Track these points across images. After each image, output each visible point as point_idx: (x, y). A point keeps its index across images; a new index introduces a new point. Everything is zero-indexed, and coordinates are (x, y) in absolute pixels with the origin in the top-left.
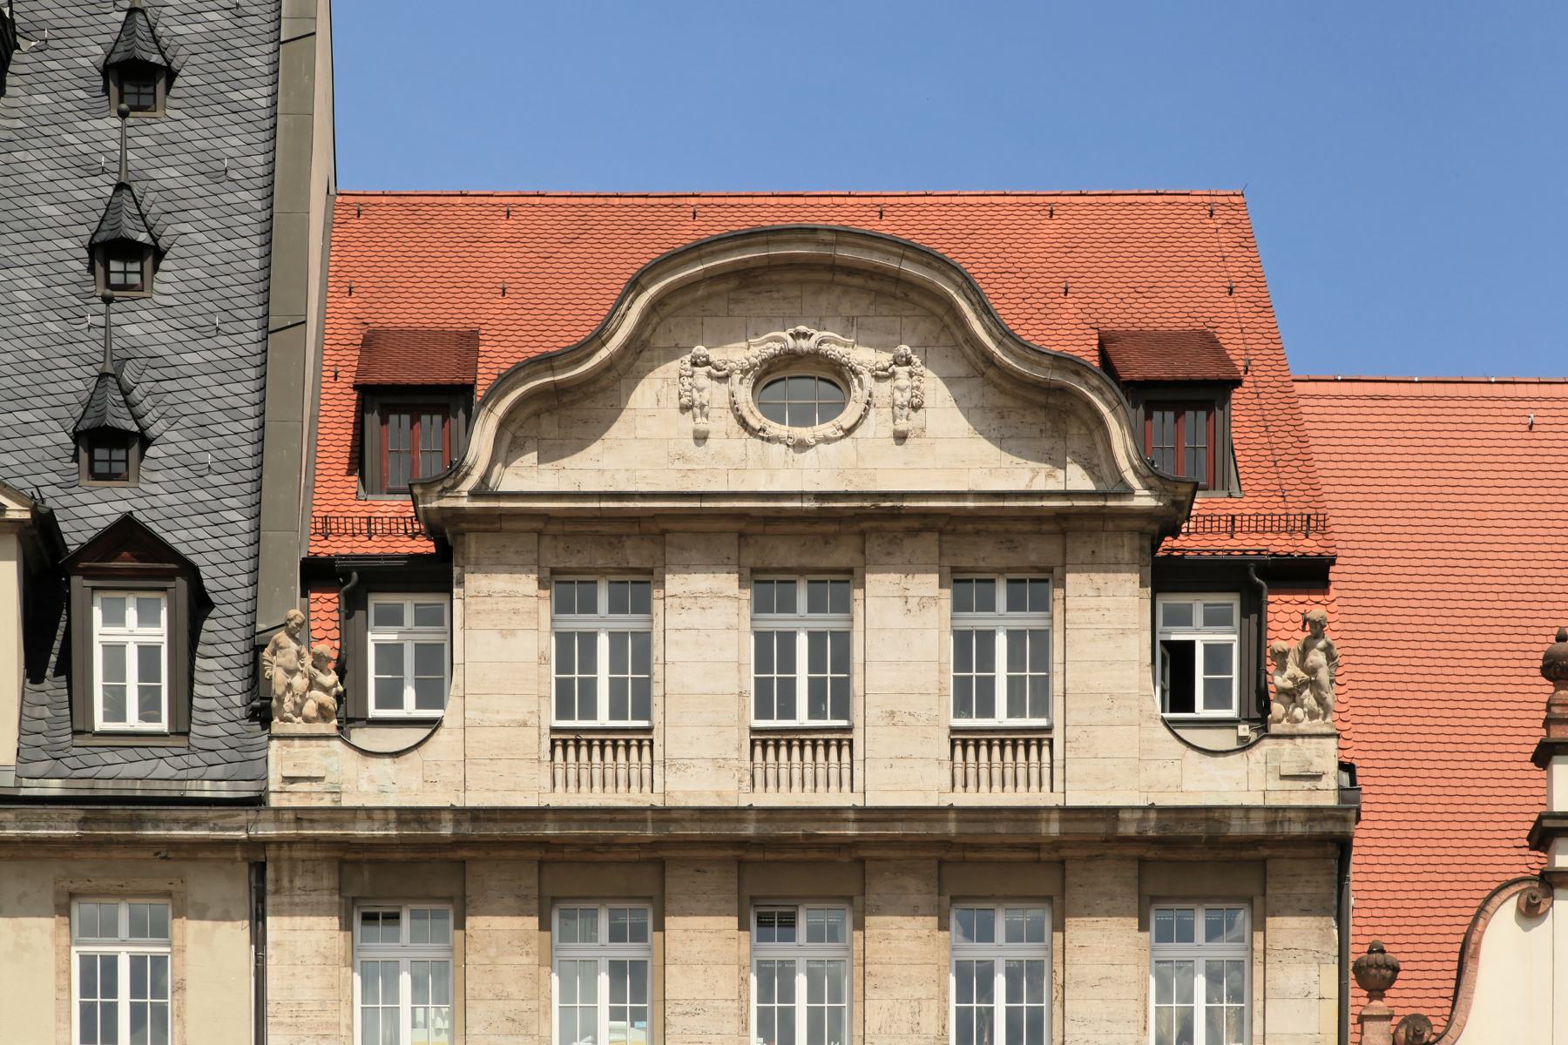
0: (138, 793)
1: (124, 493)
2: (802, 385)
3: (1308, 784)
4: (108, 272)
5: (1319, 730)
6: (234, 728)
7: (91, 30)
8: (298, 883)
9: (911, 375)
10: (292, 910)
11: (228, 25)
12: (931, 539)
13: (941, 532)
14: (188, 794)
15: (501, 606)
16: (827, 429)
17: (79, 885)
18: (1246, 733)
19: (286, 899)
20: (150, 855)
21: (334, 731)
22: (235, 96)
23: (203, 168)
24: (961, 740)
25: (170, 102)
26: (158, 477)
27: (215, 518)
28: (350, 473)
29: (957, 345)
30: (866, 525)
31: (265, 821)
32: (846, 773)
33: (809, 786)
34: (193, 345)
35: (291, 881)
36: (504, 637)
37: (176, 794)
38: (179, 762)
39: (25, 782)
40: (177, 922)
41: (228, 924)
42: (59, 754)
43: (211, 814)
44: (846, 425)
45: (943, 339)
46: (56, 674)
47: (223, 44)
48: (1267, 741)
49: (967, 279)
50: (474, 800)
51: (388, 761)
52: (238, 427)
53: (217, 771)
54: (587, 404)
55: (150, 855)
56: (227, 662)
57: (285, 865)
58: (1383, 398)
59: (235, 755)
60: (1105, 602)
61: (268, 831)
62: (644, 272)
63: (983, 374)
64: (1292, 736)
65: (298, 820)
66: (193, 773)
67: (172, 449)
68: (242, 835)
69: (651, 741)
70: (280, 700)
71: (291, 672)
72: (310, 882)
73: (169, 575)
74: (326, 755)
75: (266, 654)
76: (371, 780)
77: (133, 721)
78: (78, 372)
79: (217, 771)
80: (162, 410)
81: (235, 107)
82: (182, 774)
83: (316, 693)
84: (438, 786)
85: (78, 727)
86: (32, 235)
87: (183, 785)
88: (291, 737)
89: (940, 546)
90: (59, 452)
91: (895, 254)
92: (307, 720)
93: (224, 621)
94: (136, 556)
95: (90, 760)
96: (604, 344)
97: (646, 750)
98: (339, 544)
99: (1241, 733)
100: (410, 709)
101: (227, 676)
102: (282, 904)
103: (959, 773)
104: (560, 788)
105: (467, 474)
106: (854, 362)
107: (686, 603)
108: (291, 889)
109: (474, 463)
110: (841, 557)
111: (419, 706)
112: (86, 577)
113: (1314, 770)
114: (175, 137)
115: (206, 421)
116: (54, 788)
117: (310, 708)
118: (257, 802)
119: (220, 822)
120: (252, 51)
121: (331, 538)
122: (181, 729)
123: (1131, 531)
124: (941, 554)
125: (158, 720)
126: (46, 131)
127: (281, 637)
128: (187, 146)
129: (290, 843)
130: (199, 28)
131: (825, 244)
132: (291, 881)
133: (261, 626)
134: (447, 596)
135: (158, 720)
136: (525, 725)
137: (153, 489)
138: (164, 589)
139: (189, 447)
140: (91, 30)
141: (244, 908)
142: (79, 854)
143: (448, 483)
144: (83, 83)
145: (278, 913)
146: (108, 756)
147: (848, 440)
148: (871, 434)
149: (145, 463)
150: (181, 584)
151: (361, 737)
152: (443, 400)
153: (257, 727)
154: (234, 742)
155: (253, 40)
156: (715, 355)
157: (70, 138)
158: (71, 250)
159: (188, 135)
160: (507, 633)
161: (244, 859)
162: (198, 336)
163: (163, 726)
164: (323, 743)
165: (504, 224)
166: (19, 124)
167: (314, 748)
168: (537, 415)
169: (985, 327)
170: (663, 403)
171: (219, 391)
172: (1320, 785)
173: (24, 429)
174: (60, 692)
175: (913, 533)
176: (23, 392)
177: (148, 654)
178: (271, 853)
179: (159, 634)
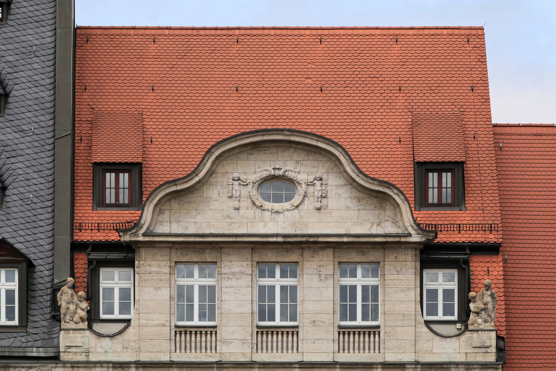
0: (7, 354)
2: (278, 185)
3: (484, 350)
5: (488, 328)
6: (45, 323)
9: (322, 184)
12: (330, 252)
13: (334, 248)
15: (155, 277)
16: (287, 205)
18: (460, 327)
21: (86, 327)
24: (343, 331)
29: (340, 172)
30: (303, 246)
31: (59, 367)
32: (295, 345)
33: (280, 351)
36: (156, 290)
37: (22, 355)
38: (24, 339)
43: (37, 365)
44: (296, 205)
45: (335, 170)
48: (467, 332)
49: (344, 149)
50: (144, 357)
51: (108, 339)
53: (39, 343)
54: (190, 195)
58: (540, 135)
60: (401, 277)
62: (213, 147)
63: (351, 184)
64: (477, 331)
66: (29, 344)
69: (216, 332)
73: (20, 262)
74: (83, 337)
75: (59, 293)
76: (102, 347)
79: (39, 343)
80: (10, 172)
82: (24, 345)
84: (129, 350)
87: (25, 350)
88: (69, 330)
89: (334, 254)
91: (315, 140)
92: (76, 323)
96: (197, 175)
97: (214, 335)
99: (458, 327)
100: (116, 315)
103: (341, 345)
104: (178, 351)
105: (141, 227)
106: (298, 180)
107: (230, 277)
109: (145, 223)
110: (293, 257)
111: (120, 314)
113: (486, 345)
117: (76, 318)
121: (83, 231)
123: (412, 248)
124: (334, 257)
131: (287, 135)
133: (56, 281)
134: (131, 270)
136: (164, 326)
143: (134, 231)
147: (296, 211)
148: (306, 208)
150: (24, 265)
151: (97, 327)
152: (129, 167)
156: (243, 177)
160: (157, 289)
162: (24, 135)
163: (16, 322)
164: (82, 332)
165: (153, 47)
167: (78, 335)
168: (170, 200)
169: (352, 169)
170: (221, 195)
172: (489, 350)
175: (323, 249)
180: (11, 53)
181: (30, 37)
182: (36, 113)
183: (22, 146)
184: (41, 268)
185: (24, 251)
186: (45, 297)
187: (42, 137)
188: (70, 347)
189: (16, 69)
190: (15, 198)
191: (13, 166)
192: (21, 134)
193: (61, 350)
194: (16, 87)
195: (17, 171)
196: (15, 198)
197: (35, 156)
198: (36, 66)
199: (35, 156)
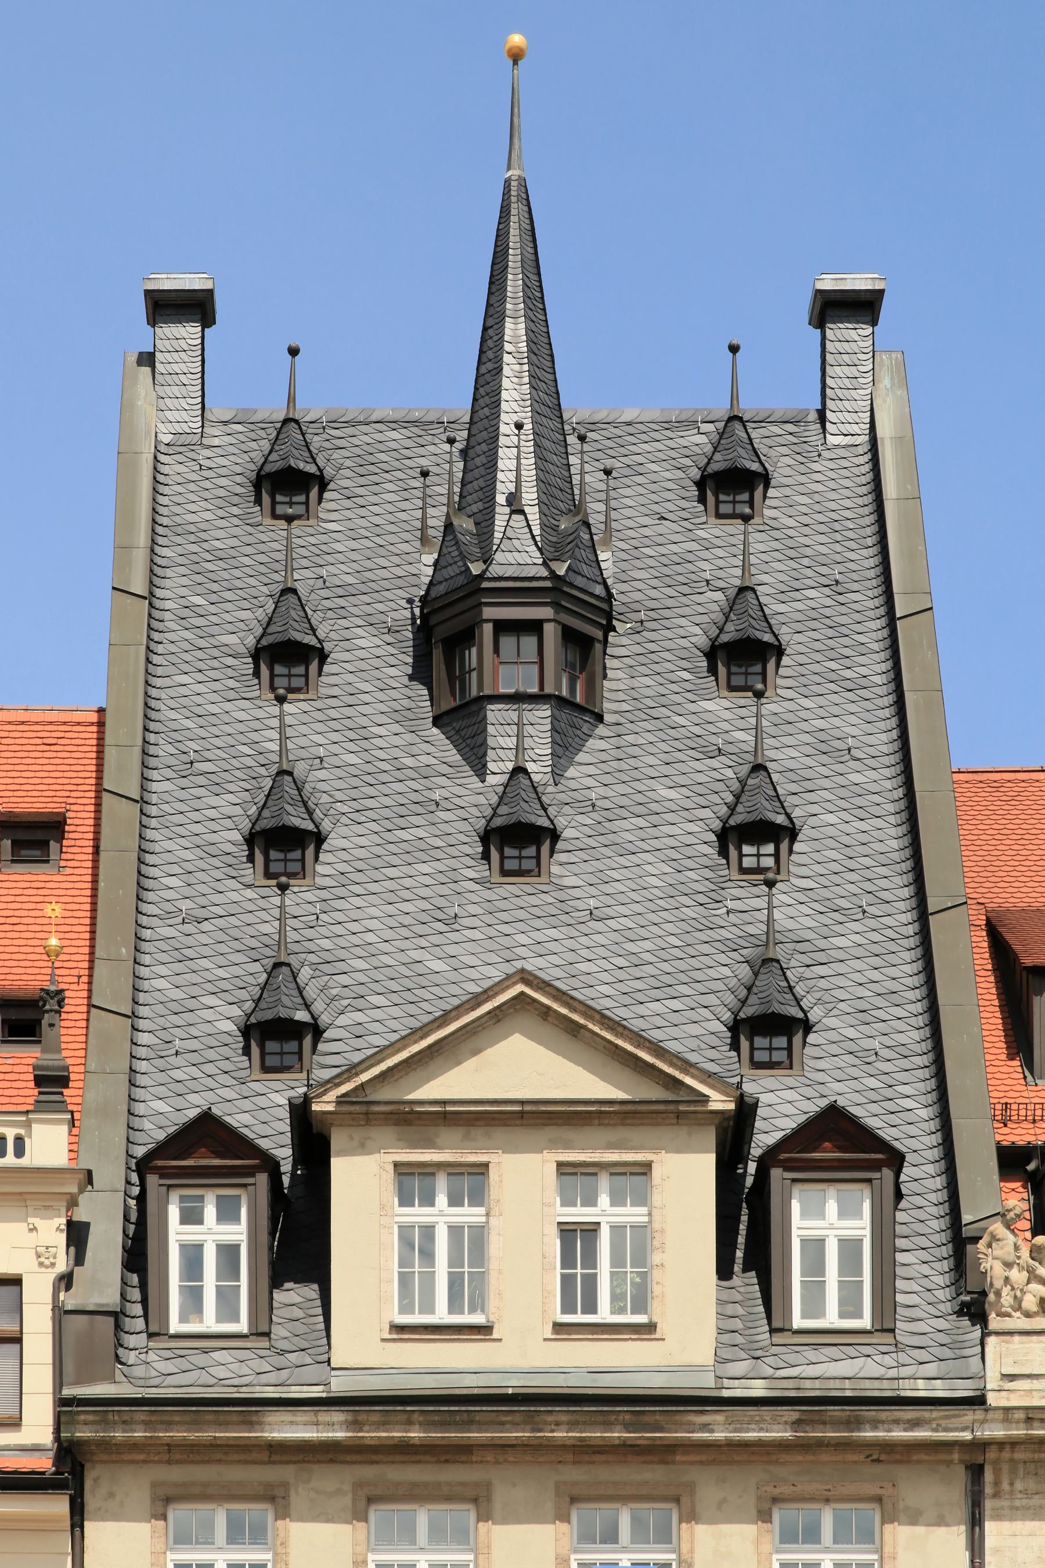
0: (848, 1393)
1: (790, 1081)
4: (741, 856)
6: (941, 1324)
7: (687, 611)
8: (1019, 1486)
10: (1015, 1513)
11: (829, 602)
14: (903, 1394)
17: (785, 1490)
19: (1006, 1503)
20: (862, 1457)
22: (848, 674)
23: (824, 747)
25: (780, 681)
26: (821, 1064)
27: (890, 1106)
28: (1011, 1057)
34: (838, 928)
35: (1012, 1484)
38: (888, 1360)
39: (726, 1383)
40: (888, 1528)
41: (942, 1530)
42: (759, 1353)
43: (935, 1414)
46: (745, 1270)
47: (827, 622)
52: (899, 1012)
55: (862, 1457)
56: (924, 1255)
57: (1005, 1468)
59: (947, 1353)
61: (996, 1431)
65: (1029, 1420)
66: (905, 1372)
67: (833, 1036)
68: (967, 1436)
70: (998, 1294)
71: (1008, 1265)
72: (1032, 1484)
77: (832, 1319)
78: (723, 958)
79: (931, 1369)
80: (818, 995)
81: (849, 685)
83: (1034, 1286)
85: (776, 1324)
86: (655, 819)
87: (895, 1384)
88: (1011, 1333)
90: (714, 1041)
92: (1028, 1315)
93: (915, 1213)
94: (840, 1144)
95: (791, 1358)
98: (1019, 1131)
101: (926, 1270)
102: (1002, 1508)
108: (1012, 1492)
112: (787, 1169)
114: (790, 717)
115: (865, 1006)
116: (758, 1389)
117: (1030, 1303)
118: (978, 1401)
119: (943, 1423)
120: (858, 628)
121: (1010, 1125)
122: (885, 1324)
125: (859, 1315)
126: (654, 713)
127: (997, 1227)
128: (804, 726)
129: (1013, 1444)
130: (799, 606)
132: (1012, 1484)
133: (966, 1218)
135: (861, 1317)
137: (820, 1077)
138: (869, 1181)
139: (851, 1033)
140: (687, 611)
141: (962, 1510)
142: (785, 1457)
144: (685, 664)
145: (998, 1517)
146: (811, 1354)
149: (808, 1050)
153: (966, 1322)
154: (943, 1338)
155: (858, 617)
157: (681, 720)
158: (698, 834)
159: (804, 714)
161: (961, 1461)
163: (865, 1322)
166: (625, 707)
171: (875, 975)
173: (675, 1018)
174: (750, 1289)
176: (668, 980)
177: (849, 1248)
178: (992, 1454)
179: (861, 1227)
181: (836, 721)
183: (838, 941)
185: (887, 1134)
186: (937, 1265)
187: (887, 921)
188: (1012, 1377)
189: (809, 785)
191: (823, 984)
192: (836, 916)
193: (988, 1387)
194: (812, 821)
195: (832, 992)
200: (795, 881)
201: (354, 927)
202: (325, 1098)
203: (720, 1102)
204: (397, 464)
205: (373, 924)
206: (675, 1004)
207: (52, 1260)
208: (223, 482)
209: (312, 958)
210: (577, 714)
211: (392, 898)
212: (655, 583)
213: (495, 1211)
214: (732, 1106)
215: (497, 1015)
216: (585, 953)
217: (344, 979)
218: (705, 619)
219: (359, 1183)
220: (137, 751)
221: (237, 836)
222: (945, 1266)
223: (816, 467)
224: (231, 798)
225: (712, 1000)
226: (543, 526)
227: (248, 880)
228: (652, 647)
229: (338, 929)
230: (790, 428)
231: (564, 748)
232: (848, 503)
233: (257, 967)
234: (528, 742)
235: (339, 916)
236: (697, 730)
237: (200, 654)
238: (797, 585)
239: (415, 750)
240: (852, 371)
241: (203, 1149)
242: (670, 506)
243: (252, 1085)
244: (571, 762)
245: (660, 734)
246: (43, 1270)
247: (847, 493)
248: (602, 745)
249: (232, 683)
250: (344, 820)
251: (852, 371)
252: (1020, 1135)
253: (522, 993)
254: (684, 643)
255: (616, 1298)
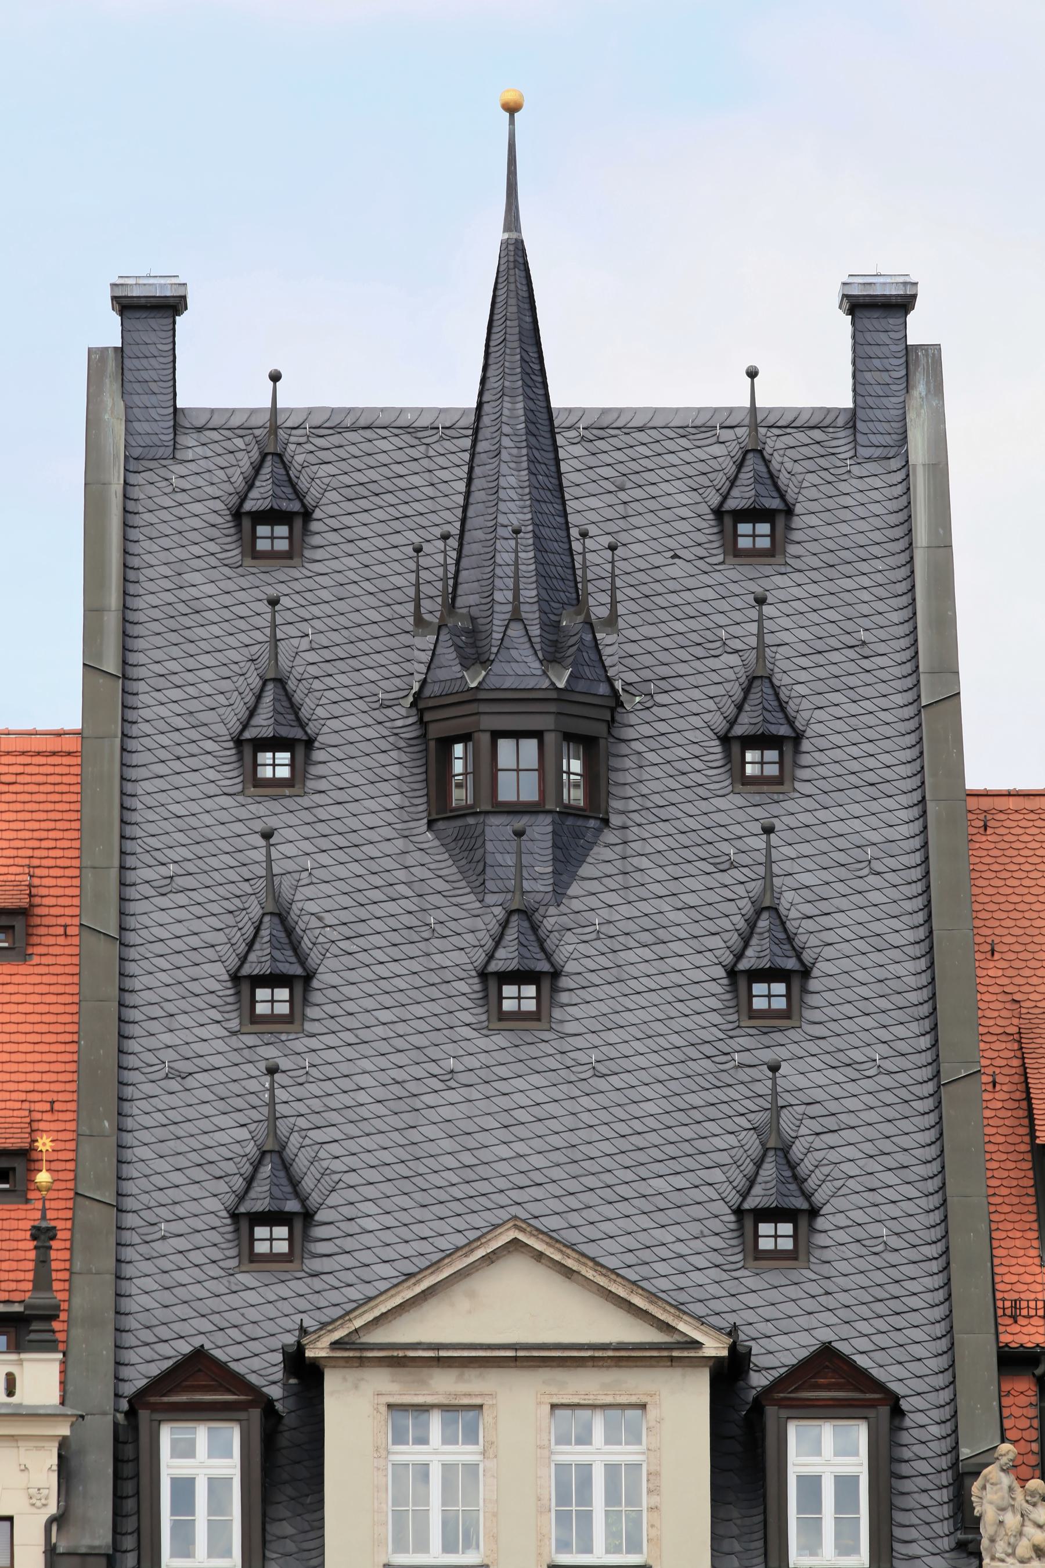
7: (701, 680)
47: (851, 694)
80: (826, 1170)
98: (1031, 1330)
112: (781, 1407)
115: (874, 1183)
121: (1022, 1321)
126: (663, 813)
128: (823, 830)
133: (965, 1452)
139: (859, 1216)
162: (855, 1075)
173: (678, 1198)
179: (858, 1465)
180: (808, 864)
181: (856, 824)
182: (883, 1019)
183: (852, 1104)
184: (921, 1419)
186: (935, 1494)
187: (903, 1078)
189: (825, 906)
190: (841, 1236)
191: (832, 1156)
192: (848, 1071)
194: (828, 952)
195: (842, 1166)
196: (841, 1236)
197: (888, 1129)
198: (875, 897)
199: (888, 1129)
200: (807, 1027)
201: (346, 1084)
202: (319, 1345)
203: (715, 1347)
204: (387, 484)
205: (365, 1080)
206: (679, 1182)
207: (43, 1501)
208: (198, 508)
209: (302, 1123)
210: (578, 827)
211: (384, 1047)
212: (667, 643)
213: (491, 1453)
214: (725, 1353)
215: (490, 1259)
216: (586, 1117)
217: (335, 1149)
218: (719, 690)
219: (351, 1413)
220: (114, 873)
221: (219, 970)
222: (945, 1495)
223: (844, 487)
224: (214, 922)
225: (716, 1176)
226: (543, 625)
227: (234, 1025)
228: (662, 727)
229: (329, 1087)
230: (817, 434)
231: (567, 858)
232: (877, 536)
233: (243, 1134)
234: (526, 859)
235: (330, 1071)
236: (708, 835)
237: (177, 737)
238: (820, 645)
239: (409, 860)
240: (885, 377)
241: (197, 1383)
242: (684, 540)
243: (240, 1277)
244: (574, 876)
245: (669, 840)
246: (34, 1510)
247: (878, 523)
248: (607, 854)
249: (212, 774)
250: (334, 949)
251: (885, 377)
252: (1031, 1334)
253: (515, 1241)
254: (696, 721)
255: (612, 1534)
